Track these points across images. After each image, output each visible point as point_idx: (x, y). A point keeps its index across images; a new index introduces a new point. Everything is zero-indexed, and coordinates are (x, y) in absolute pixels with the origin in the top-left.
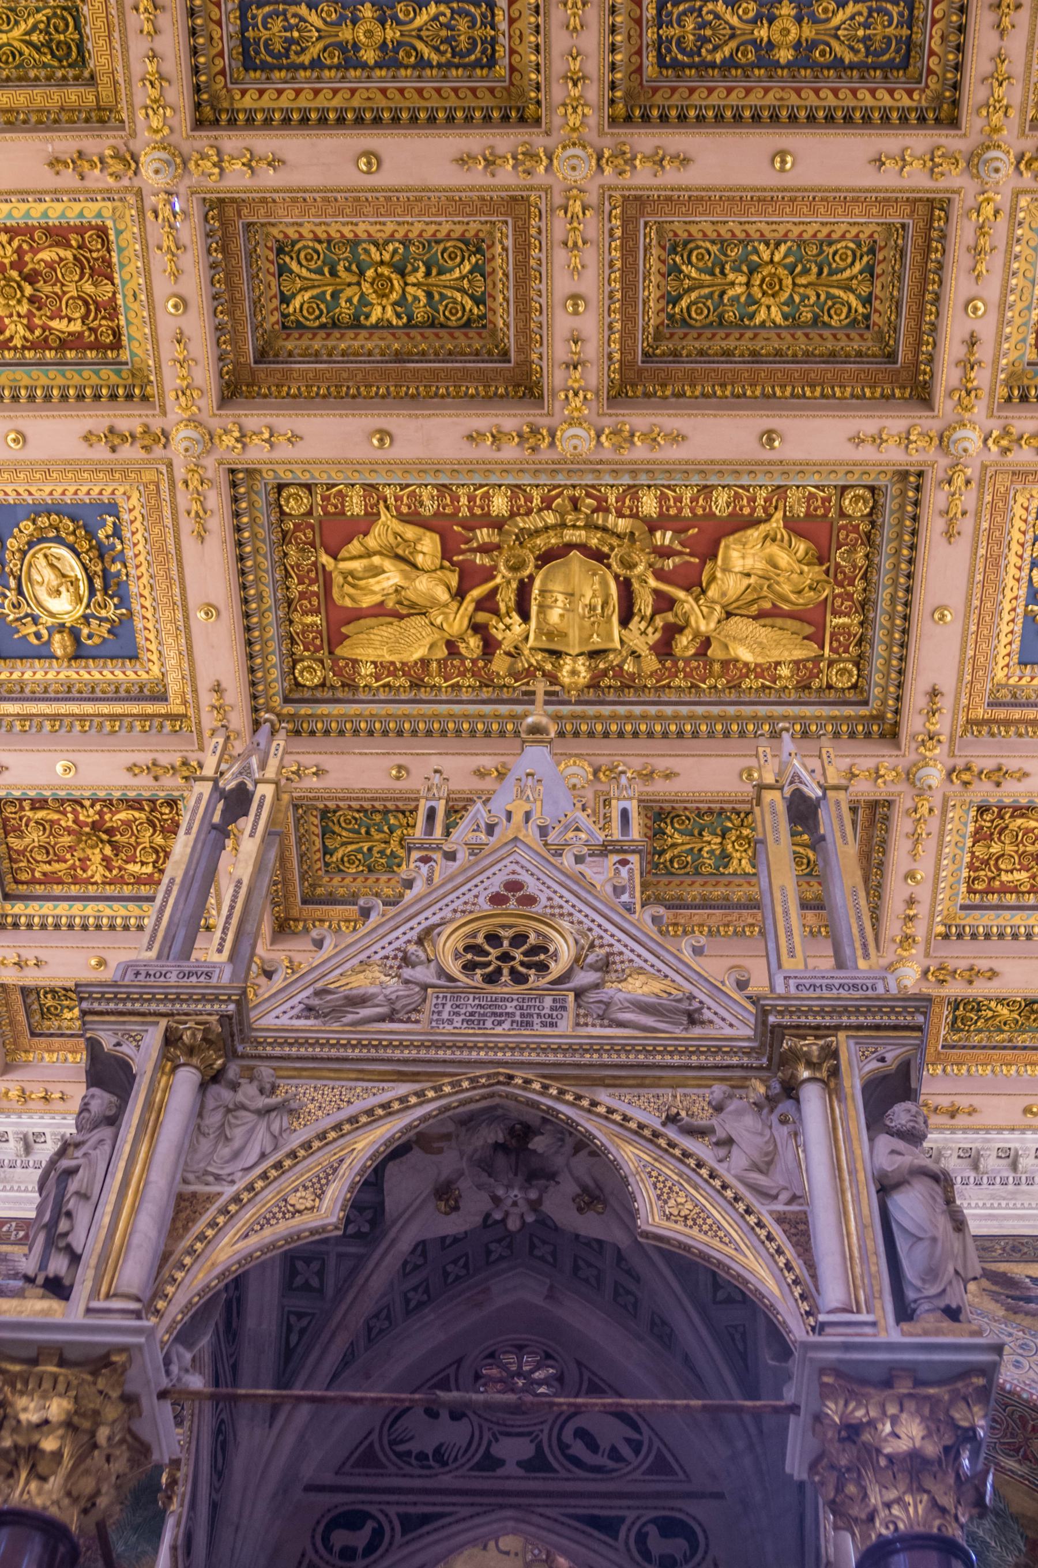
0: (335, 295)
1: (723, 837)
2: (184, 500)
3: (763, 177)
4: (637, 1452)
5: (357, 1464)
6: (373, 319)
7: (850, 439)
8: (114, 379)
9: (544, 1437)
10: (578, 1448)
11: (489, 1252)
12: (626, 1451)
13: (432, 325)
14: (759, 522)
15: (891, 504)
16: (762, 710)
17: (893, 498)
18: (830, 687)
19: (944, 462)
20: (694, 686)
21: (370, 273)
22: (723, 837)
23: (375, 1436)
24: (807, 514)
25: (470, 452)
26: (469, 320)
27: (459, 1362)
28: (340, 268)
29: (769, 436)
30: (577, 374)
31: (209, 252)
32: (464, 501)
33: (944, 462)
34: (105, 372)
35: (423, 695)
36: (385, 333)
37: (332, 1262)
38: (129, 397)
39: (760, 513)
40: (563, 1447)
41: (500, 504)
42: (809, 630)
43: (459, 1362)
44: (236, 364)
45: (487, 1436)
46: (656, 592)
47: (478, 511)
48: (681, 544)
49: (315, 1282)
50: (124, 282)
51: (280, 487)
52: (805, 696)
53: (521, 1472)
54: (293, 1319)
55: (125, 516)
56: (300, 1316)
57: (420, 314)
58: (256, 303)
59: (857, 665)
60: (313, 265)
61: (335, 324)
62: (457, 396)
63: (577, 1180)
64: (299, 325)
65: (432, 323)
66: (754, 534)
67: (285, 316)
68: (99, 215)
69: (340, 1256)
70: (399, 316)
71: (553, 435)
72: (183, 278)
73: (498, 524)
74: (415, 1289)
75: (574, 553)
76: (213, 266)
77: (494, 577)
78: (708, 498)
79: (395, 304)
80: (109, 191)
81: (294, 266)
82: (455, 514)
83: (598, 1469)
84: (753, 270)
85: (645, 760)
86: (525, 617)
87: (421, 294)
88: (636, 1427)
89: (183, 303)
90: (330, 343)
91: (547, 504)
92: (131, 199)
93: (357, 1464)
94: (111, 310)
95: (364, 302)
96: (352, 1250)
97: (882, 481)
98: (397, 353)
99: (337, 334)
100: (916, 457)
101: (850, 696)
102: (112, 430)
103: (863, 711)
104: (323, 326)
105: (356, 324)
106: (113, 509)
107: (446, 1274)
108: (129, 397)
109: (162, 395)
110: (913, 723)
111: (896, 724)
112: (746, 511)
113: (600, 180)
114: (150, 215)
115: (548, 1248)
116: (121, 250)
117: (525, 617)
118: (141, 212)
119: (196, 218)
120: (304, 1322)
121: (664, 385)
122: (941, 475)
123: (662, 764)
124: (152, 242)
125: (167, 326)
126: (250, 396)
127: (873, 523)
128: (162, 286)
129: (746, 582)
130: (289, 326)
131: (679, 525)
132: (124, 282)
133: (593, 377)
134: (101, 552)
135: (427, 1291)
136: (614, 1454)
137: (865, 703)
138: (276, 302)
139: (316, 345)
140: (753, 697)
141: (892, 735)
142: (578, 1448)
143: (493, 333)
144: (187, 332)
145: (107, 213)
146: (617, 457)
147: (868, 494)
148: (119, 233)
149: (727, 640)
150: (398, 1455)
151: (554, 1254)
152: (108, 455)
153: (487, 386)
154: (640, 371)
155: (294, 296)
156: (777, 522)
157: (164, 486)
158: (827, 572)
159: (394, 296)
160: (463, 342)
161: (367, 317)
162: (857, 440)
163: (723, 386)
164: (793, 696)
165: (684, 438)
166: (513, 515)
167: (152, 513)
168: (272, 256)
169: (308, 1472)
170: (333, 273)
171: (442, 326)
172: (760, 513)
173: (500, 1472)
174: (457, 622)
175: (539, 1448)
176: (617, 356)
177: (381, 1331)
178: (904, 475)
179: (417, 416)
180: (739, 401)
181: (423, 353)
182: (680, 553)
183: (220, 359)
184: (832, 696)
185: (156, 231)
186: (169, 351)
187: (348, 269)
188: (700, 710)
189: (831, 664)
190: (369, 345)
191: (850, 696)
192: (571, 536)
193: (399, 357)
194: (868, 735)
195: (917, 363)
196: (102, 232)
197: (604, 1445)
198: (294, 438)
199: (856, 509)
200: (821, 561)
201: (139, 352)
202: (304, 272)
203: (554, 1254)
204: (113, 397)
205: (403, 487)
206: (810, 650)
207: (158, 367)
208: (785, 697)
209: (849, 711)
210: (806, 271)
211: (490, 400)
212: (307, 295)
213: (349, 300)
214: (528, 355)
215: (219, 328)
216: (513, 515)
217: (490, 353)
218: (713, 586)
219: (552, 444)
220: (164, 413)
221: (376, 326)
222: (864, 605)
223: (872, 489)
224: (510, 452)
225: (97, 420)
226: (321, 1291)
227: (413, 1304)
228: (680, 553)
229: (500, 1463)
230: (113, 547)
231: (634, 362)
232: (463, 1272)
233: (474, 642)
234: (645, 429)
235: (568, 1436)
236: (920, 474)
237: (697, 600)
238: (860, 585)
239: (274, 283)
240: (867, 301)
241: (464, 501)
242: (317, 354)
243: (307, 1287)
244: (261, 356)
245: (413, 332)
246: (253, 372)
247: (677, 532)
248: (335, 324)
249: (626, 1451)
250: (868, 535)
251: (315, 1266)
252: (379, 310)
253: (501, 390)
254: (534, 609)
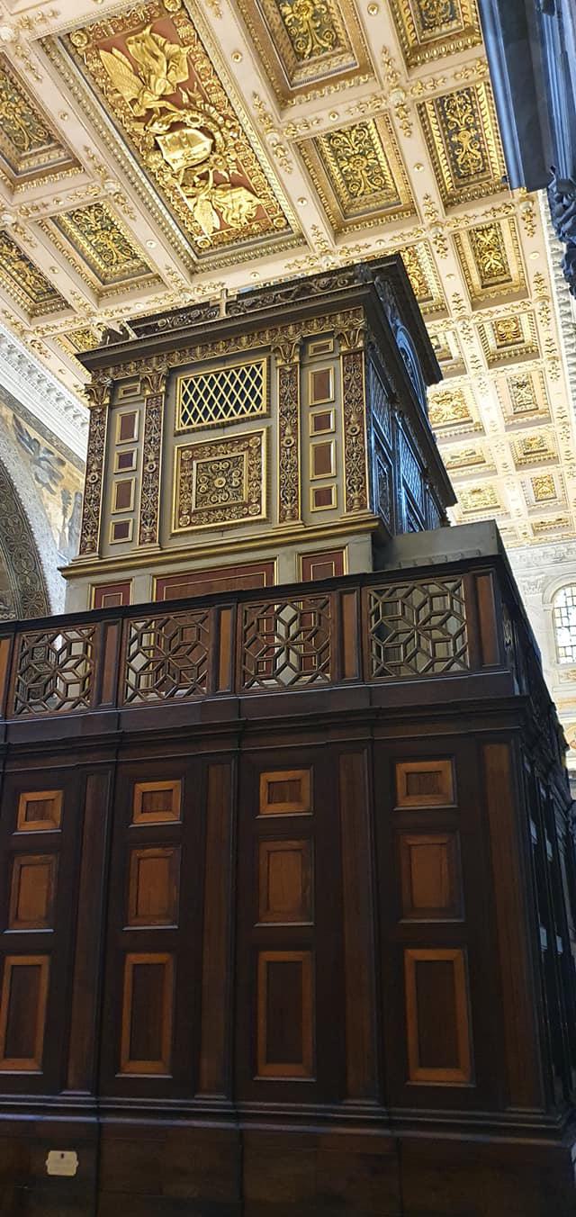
1: (102, 229)
3: (410, 162)
14: (255, 195)
18: (196, 242)
19: (317, 255)
22: (102, 229)
25: (248, 97)
29: (302, 200)
33: (317, 255)
35: (100, 96)
39: (260, 193)
42: (218, 227)
46: (207, 172)
66: (251, 196)
75: (212, 141)
84: (363, 154)
85: (134, 207)
86: (170, 131)
91: (226, 118)
103: (195, 259)
113: (392, 108)
117: (170, 131)
123: (136, 213)
137: (198, 257)
141: (193, 273)
146: (271, 154)
149: (199, 205)
174: (151, 101)
178: (301, 236)
179: (256, 69)
192: (217, 135)
195: (347, 226)
209: (192, 255)
210: (368, 171)
214: (298, 94)
218: (220, 192)
233: (143, 112)
236: (306, 243)
240: (362, 194)
253: (278, 91)
254: (177, 134)
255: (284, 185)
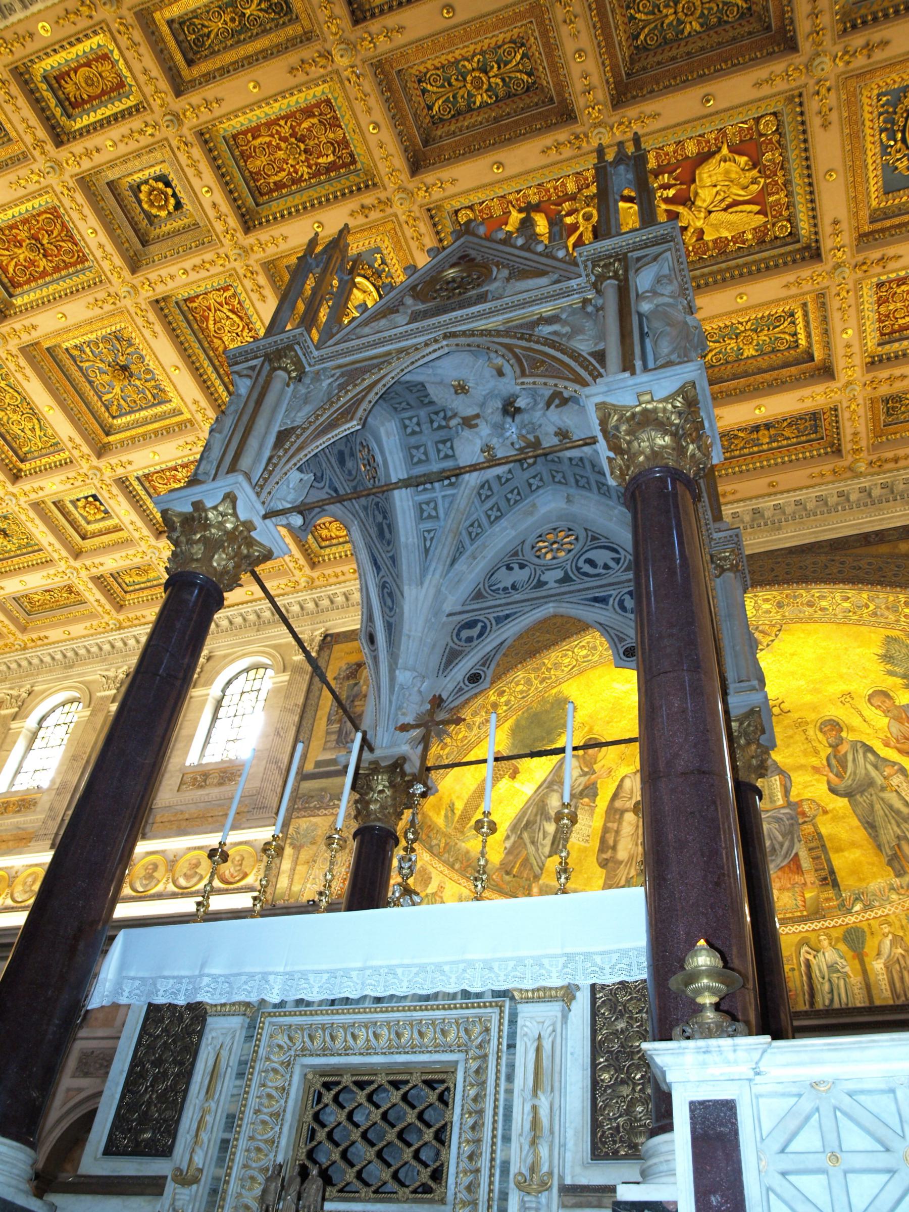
0: (454, 97)
2: (409, 232)
4: (618, 563)
5: (473, 599)
6: (478, 104)
7: (754, 85)
8: (357, 180)
9: (568, 567)
10: (587, 568)
11: (530, 485)
12: (612, 564)
13: (509, 97)
14: (715, 153)
15: (787, 119)
16: (740, 261)
17: (788, 115)
18: (776, 238)
20: (701, 258)
21: (469, 78)
23: (481, 586)
24: (741, 141)
26: (528, 88)
27: (523, 542)
28: (452, 80)
30: (591, 97)
31: (383, 93)
32: (552, 190)
34: (352, 177)
36: (486, 109)
37: (440, 501)
38: (367, 187)
40: (578, 569)
41: (571, 187)
42: (756, 208)
43: (523, 542)
44: (415, 151)
45: (539, 572)
46: (666, 211)
47: (561, 194)
48: (675, 179)
49: (433, 513)
50: (346, 125)
51: (456, 212)
52: (763, 247)
53: (557, 585)
54: (426, 534)
55: (385, 252)
56: (429, 531)
57: (501, 94)
58: (415, 115)
59: (789, 221)
60: (439, 84)
61: (459, 113)
62: (532, 131)
63: (553, 424)
64: (441, 120)
65: (509, 95)
66: (714, 161)
67: (432, 117)
68: (323, 93)
69: (444, 497)
70: (490, 97)
71: (586, 136)
72: (373, 112)
73: (573, 198)
74: (491, 509)
76: (387, 100)
77: (578, 228)
78: (683, 148)
79: (486, 91)
80: (323, 76)
81: (429, 87)
82: (549, 199)
83: (598, 575)
87: (499, 81)
88: (617, 552)
89: (377, 126)
90: (459, 125)
92: (335, 77)
93: (473, 599)
94: (343, 143)
95: (470, 95)
96: (449, 492)
97: (779, 107)
98: (495, 118)
99: (461, 118)
100: (793, 84)
101: (789, 240)
102: (363, 207)
103: (798, 246)
104: (453, 116)
105: (470, 109)
106: (378, 250)
107: (508, 500)
108: (367, 187)
109: (381, 180)
110: (827, 244)
111: (818, 248)
112: (706, 149)
114: (347, 83)
115: (560, 475)
116: (340, 108)
118: (342, 82)
119: (370, 77)
120: (432, 534)
121: (641, 89)
122: (811, 91)
124: (352, 98)
125: (373, 142)
126: (426, 166)
127: (780, 134)
128: (364, 119)
129: (715, 190)
130: (437, 121)
131: (670, 168)
132: (346, 125)
133: (601, 94)
134: (378, 274)
135: (499, 510)
136: (606, 567)
137: (798, 241)
138: (425, 111)
139: (453, 128)
140: (735, 256)
142: (587, 568)
143: (542, 90)
144: (384, 141)
145: (327, 91)
147: (772, 118)
148: (336, 99)
150: (493, 591)
151: (564, 477)
152: (365, 220)
153: (546, 121)
154: (627, 85)
155: (434, 104)
156: (725, 151)
157: (398, 230)
158: (759, 172)
159: (485, 87)
160: (528, 101)
161: (475, 103)
162: (758, 85)
163: (675, 78)
164: (757, 249)
165: (659, 115)
166: (580, 190)
167: (398, 246)
168: (416, 86)
169: (448, 607)
170: (450, 85)
171: (515, 95)
172: (714, 149)
173: (545, 587)
175: (566, 573)
176: (611, 80)
177: (477, 534)
178: (790, 99)
180: (686, 83)
181: (509, 114)
182: (675, 185)
183: (406, 151)
184: (779, 242)
185: (353, 91)
186: (378, 153)
187: (457, 80)
188: (706, 270)
189: (774, 225)
190: (480, 119)
191: (789, 240)
193: (496, 120)
194: (803, 259)
196: (328, 102)
197: (600, 563)
198: (454, 181)
199: (768, 127)
200: (754, 166)
201: (365, 161)
202: (435, 89)
203: (564, 477)
204: (359, 189)
205: (518, 192)
206: (761, 219)
207: (375, 165)
208: (752, 251)
209: (789, 248)
211: (549, 128)
212: (440, 102)
213: (462, 97)
215: (400, 134)
216: (580, 190)
217: (543, 102)
219: (588, 142)
220: (385, 189)
221: (480, 107)
222: (787, 183)
223: (775, 114)
224: (567, 152)
225: (353, 204)
226: (437, 517)
227: (493, 518)
228: (675, 185)
229: (546, 583)
230: (384, 270)
231: (622, 80)
232: (518, 498)
234: (636, 116)
235: (581, 563)
237: (690, 209)
238: (780, 173)
239: (421, 99)
241: (552, 190)
242: (454, 132)
243: (430, 517)
244: (426, 143)
245: (500, 104)
246: (424, 153)
247: (670, 173)
248: (459, 113)
249: (612, 564)
250: (779, 142)
251: (432, 505)
252: (479, 98)
255: (678, 125)
